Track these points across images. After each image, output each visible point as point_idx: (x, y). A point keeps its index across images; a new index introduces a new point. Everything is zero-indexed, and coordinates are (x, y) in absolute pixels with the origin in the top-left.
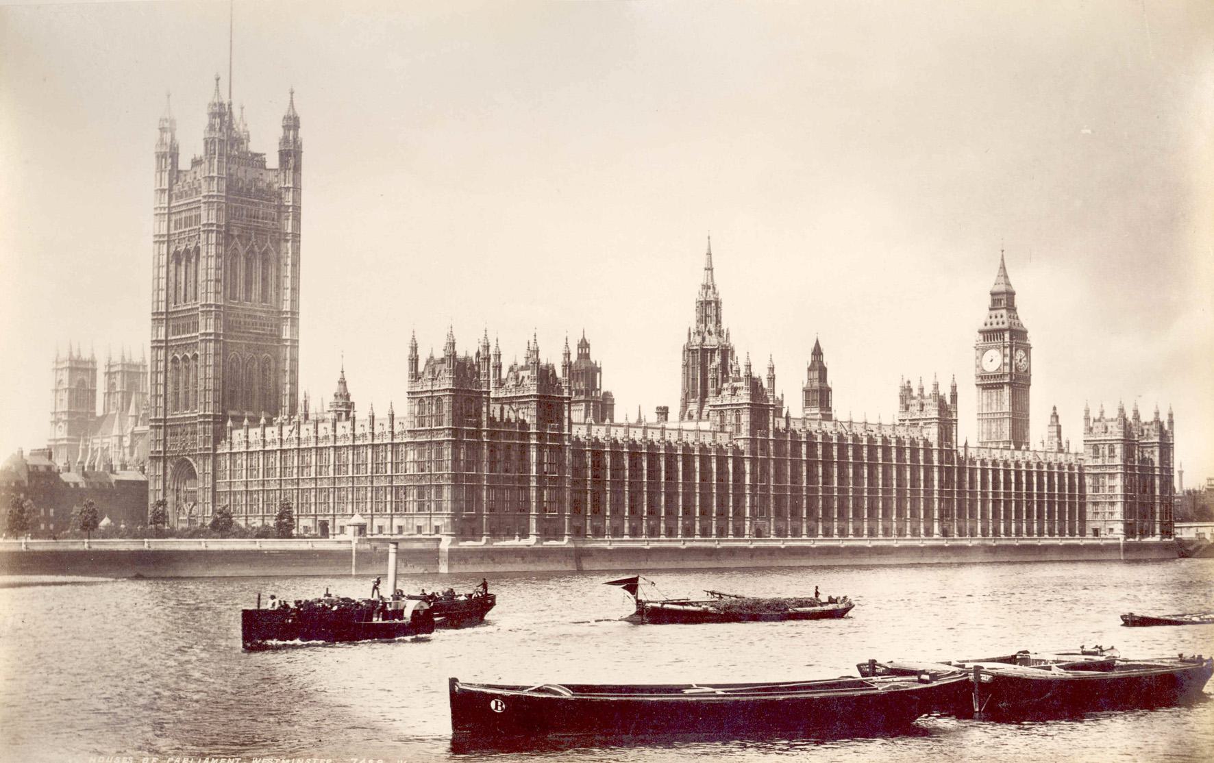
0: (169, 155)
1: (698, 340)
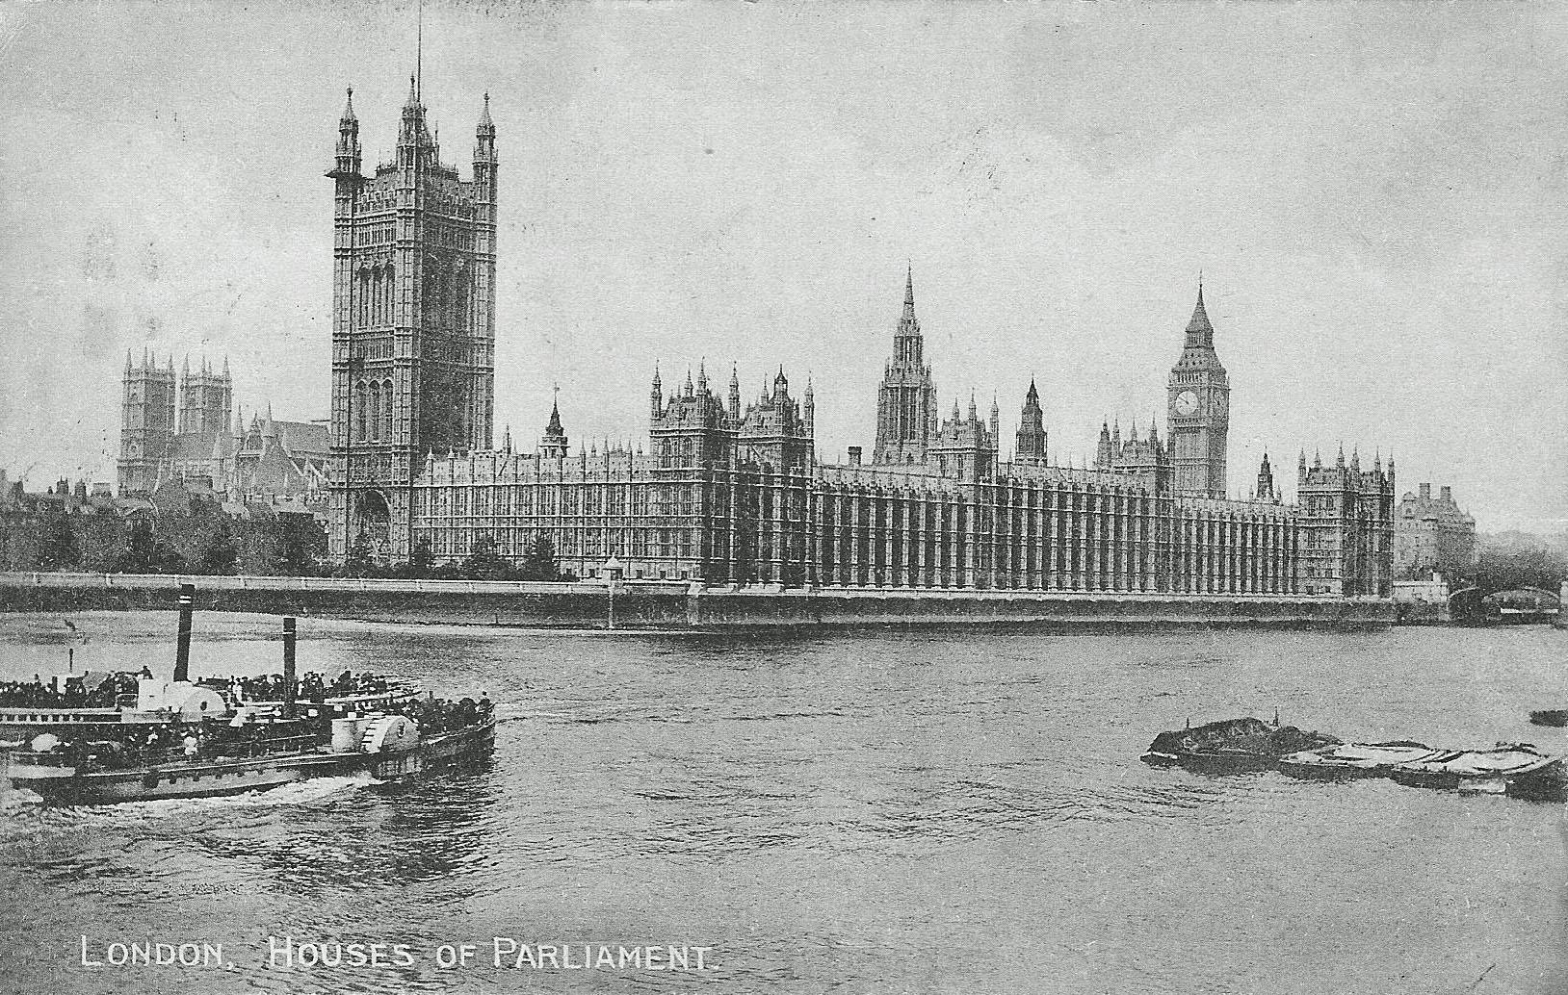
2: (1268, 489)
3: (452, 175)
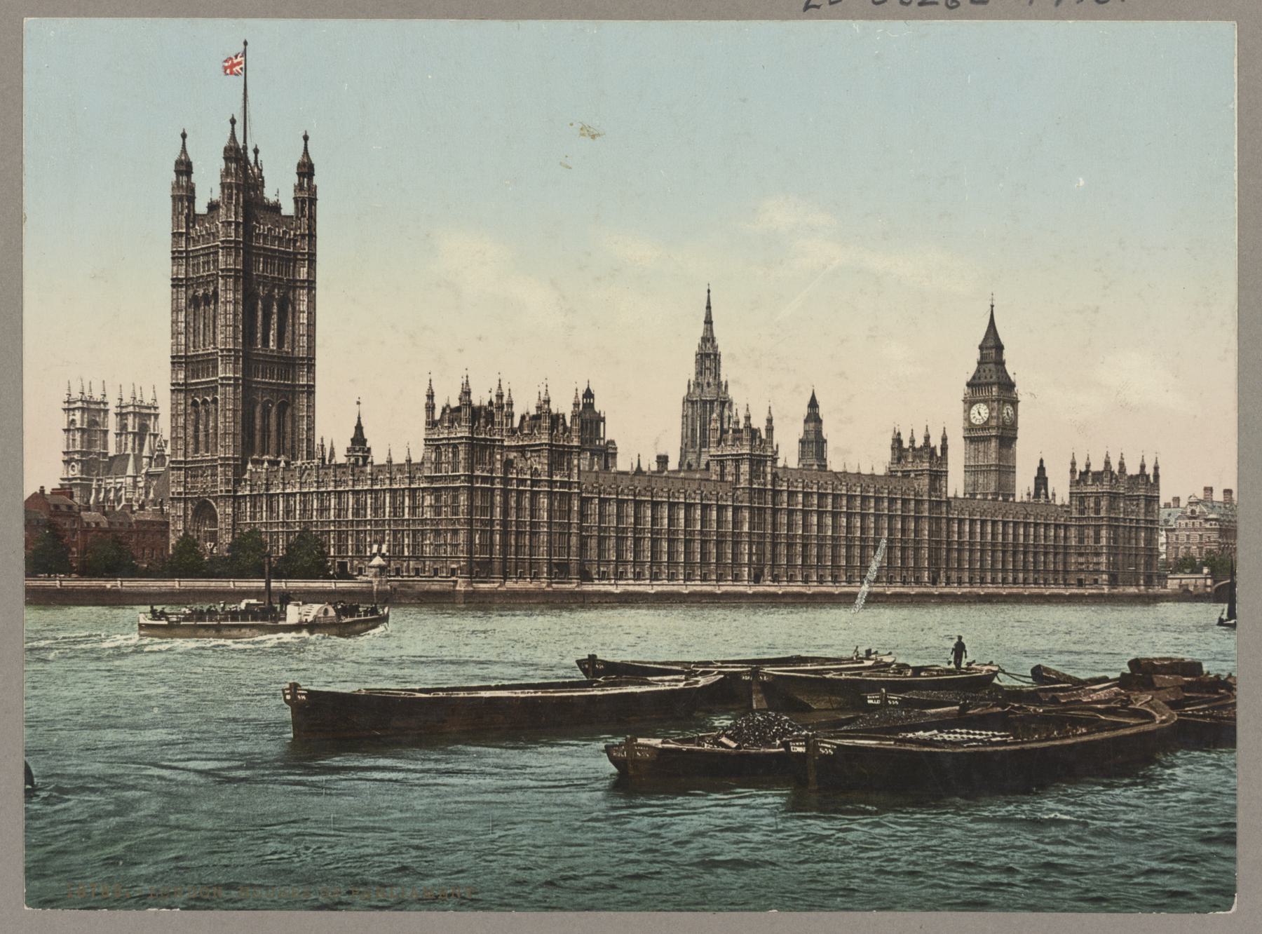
2: (1043, 491)
3: (276, 208)
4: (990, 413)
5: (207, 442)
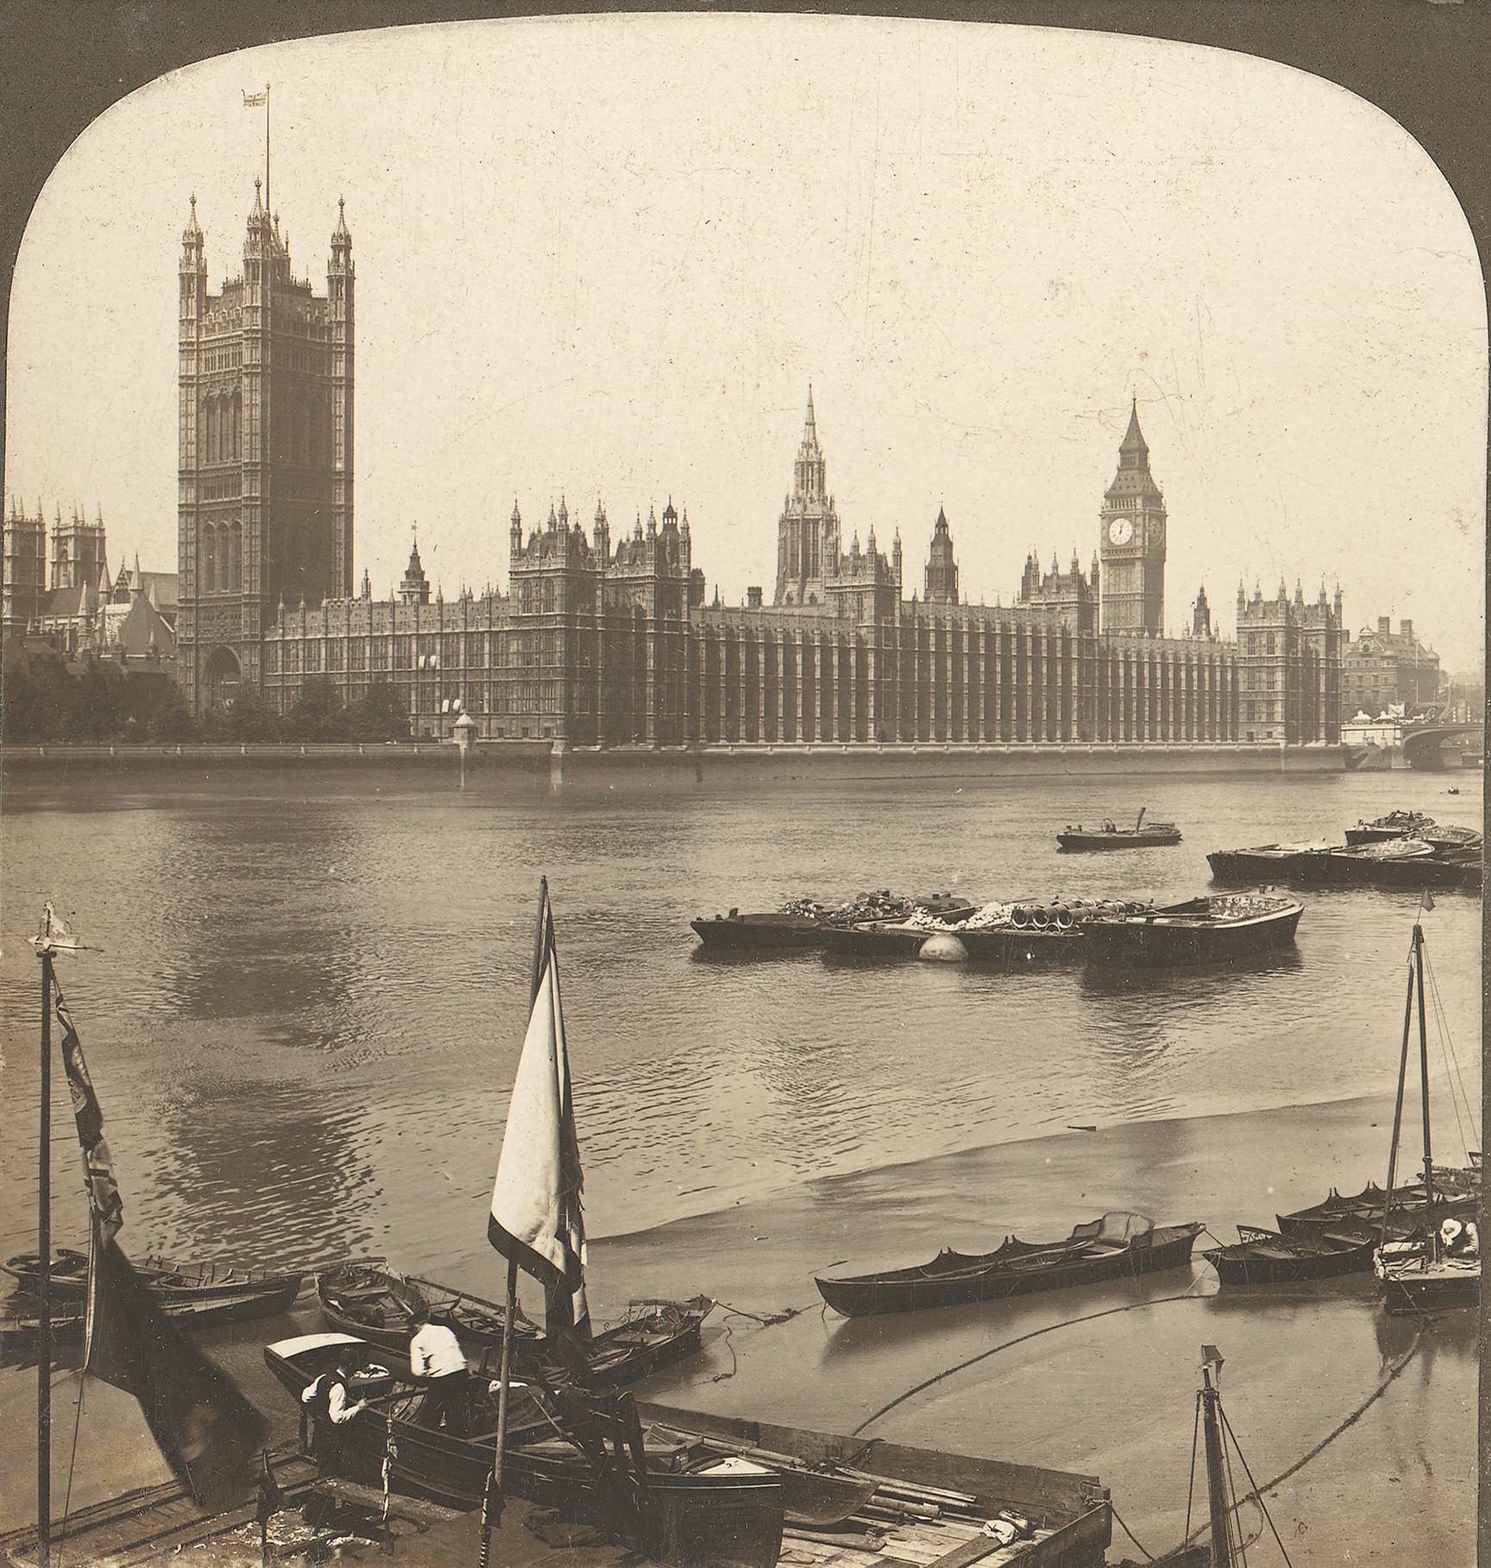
0: (193, 282)
1: (799, 508)
2: (1204, 626)
3: (305, 290)
4: (1134, 531)
5: (225, 576)
